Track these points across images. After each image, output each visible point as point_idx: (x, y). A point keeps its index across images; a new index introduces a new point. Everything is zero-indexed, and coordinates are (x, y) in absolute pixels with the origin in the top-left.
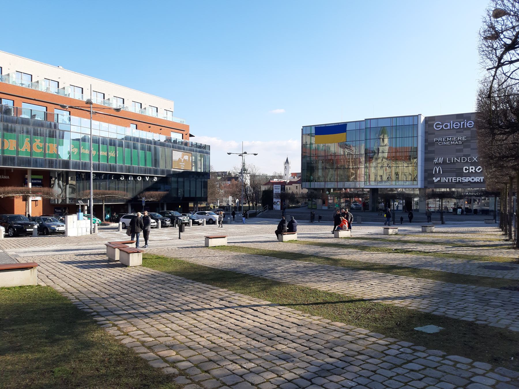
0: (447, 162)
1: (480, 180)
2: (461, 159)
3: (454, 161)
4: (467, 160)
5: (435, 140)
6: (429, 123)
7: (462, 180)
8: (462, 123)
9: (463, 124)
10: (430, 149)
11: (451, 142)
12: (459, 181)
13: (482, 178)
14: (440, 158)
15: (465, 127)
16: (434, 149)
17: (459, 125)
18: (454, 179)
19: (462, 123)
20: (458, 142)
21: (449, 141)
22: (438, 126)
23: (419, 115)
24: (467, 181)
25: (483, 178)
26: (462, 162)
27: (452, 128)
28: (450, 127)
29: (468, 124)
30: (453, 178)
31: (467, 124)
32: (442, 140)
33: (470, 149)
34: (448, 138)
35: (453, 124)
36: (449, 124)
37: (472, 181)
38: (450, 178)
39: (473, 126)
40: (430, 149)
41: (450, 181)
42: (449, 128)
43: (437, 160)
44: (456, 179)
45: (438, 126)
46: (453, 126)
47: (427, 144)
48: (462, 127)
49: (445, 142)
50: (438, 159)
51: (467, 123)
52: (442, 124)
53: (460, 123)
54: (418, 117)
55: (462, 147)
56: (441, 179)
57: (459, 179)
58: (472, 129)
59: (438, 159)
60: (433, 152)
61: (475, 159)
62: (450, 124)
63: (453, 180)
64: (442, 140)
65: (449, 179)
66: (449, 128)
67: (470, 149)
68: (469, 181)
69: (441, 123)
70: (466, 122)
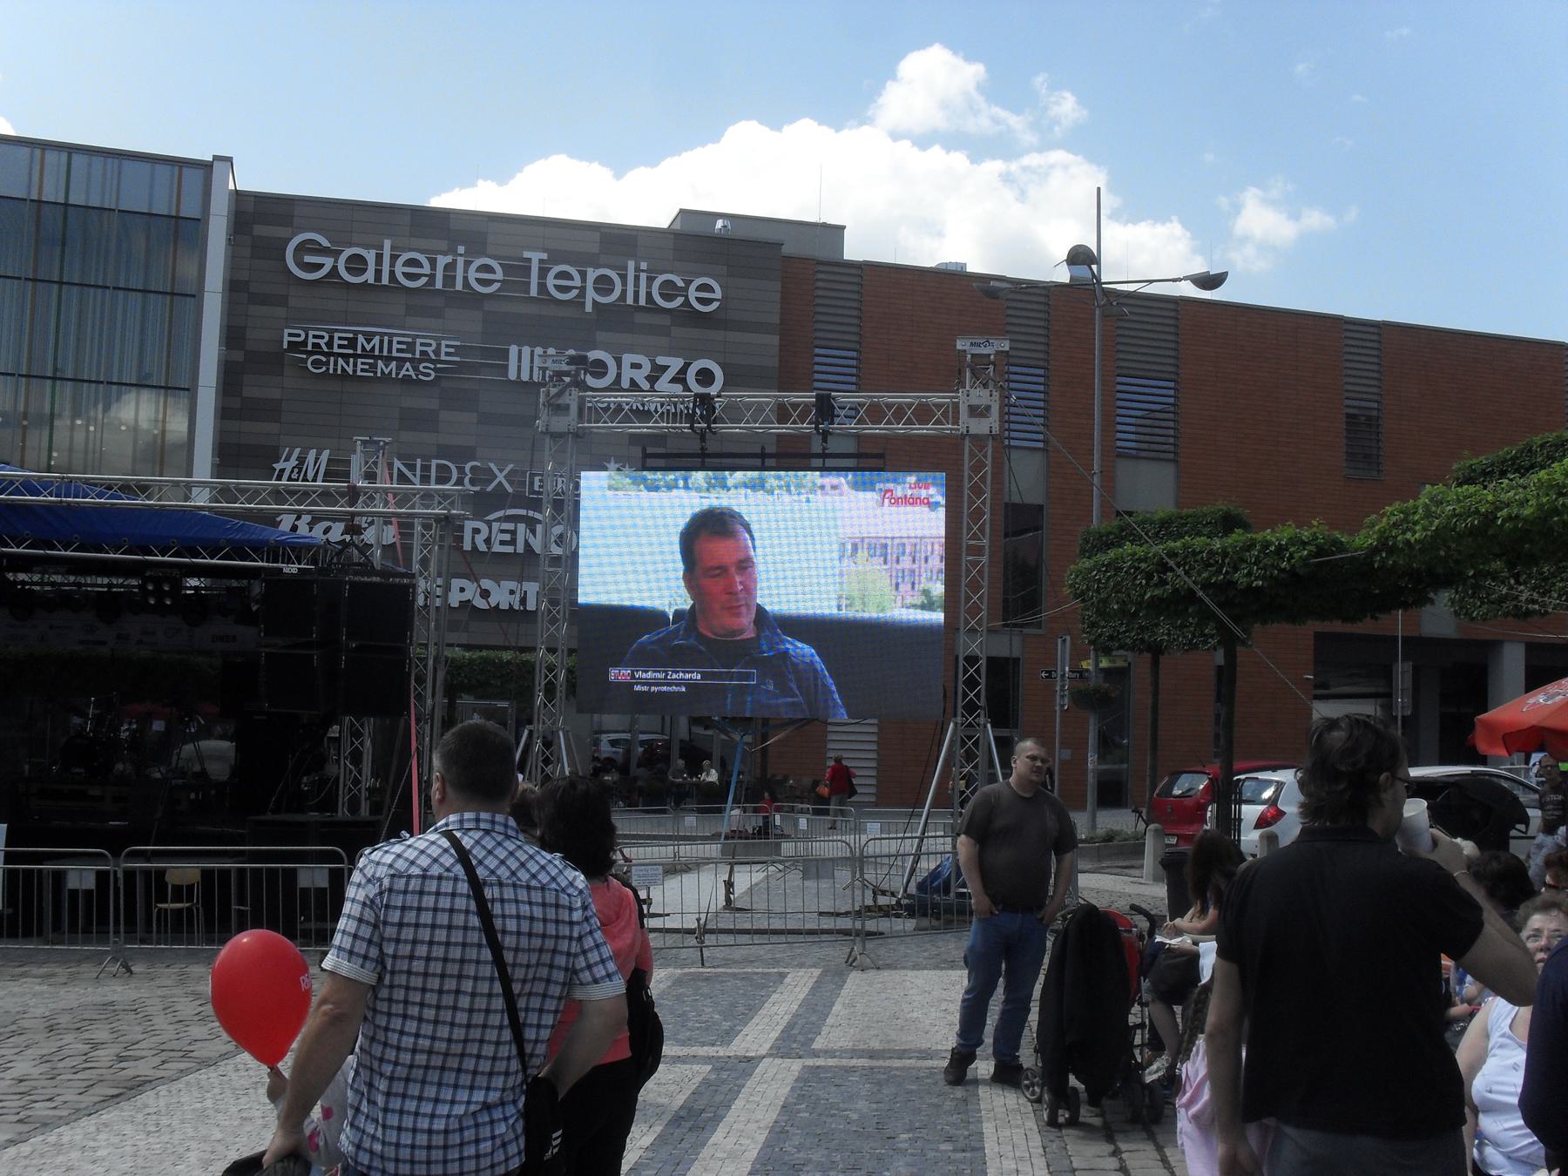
1: (523, 601)
2: (426, 468)
5: (286, 339)
6: (261, 230)
8: (442, 261)
9: (450, 267)
10: (256, 388)
11: (380, 363)
15: (459, 286)
16: (276, 394)
17: (427, 270)
19: (442, 261)
20: (416, 369)
21: (366, 354)
22: (308, 259)
23: (216, 157)
28: (378, 273)
31: (466, 271)
32: (330, 344)
34: (361, 339)
35: (394, 258)
36: (370, 256)
37: (480, 603)
39: (496, 286)
40: (256, 388)
42: (369, 276)
43: (293, 462)
45: (308, 259)
46: (392, 273)
47: (238, 356)
48: (439, 285)
49: (345, 357)
50: (301, 460)
51: (467, 264)
52: (338, 253)
53: (433, 263)
54: (206, 170)
55: (434, 404)
59: (301, 460)
60: (268, 410)
61: (501, 477)
62: (379, 257)
64: (330, 344)
66: (369, 276)
70: (461, 261)
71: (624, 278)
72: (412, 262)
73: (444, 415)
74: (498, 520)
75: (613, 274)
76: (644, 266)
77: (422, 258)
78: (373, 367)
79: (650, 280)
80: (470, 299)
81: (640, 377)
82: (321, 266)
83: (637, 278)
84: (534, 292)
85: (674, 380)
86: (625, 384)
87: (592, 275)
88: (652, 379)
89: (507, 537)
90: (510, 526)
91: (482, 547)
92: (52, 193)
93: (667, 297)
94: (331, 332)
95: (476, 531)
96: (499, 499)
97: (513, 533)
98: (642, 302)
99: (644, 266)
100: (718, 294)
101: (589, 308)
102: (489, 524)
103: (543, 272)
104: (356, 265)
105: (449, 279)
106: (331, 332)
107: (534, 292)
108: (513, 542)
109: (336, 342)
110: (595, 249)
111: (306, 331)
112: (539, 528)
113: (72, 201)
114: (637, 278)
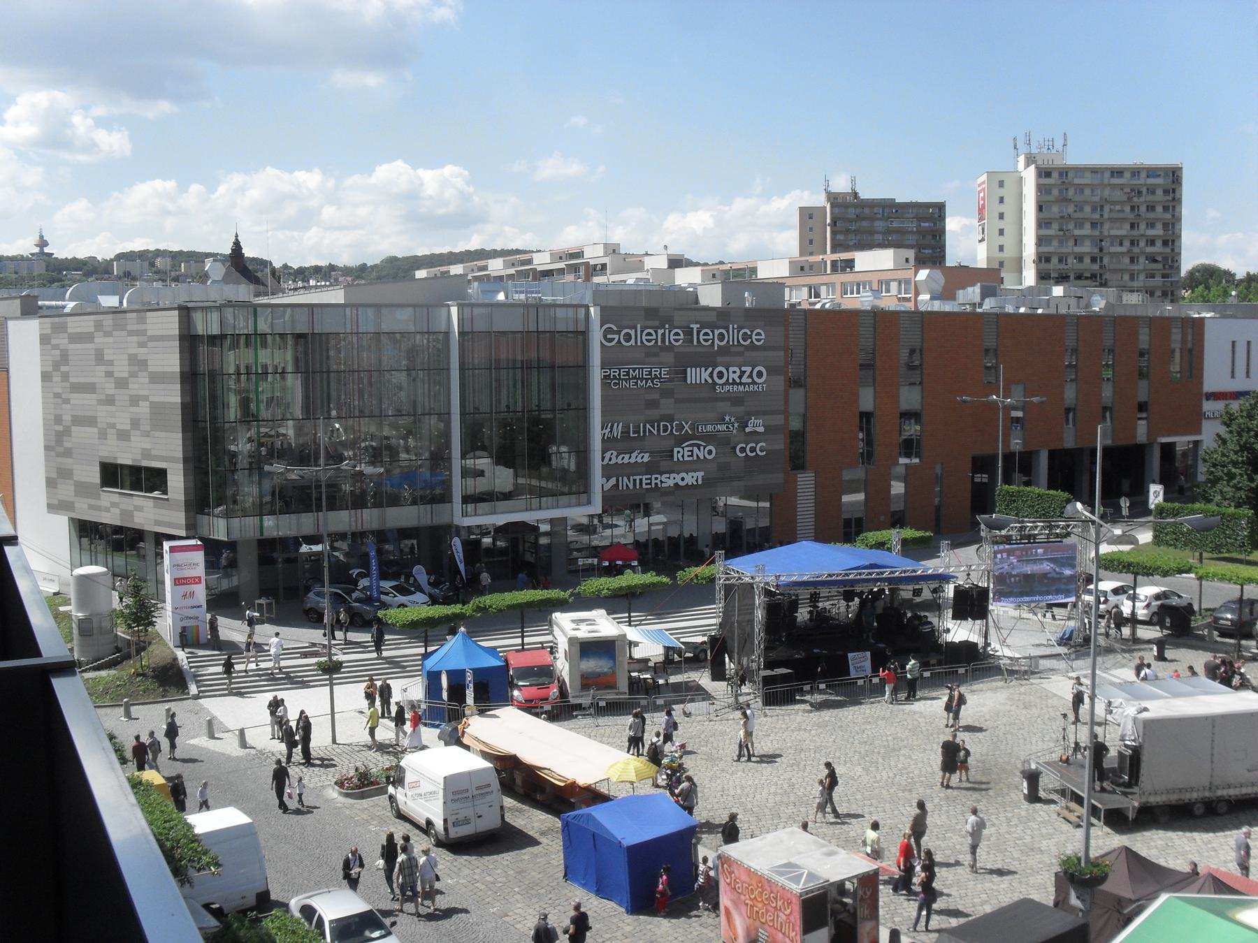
0: (632, 435)
1: (697, 481)
3: (644, 432)
4: (671, 431)
9: (663, 335)
12: (656, 484)
13: (700, 474)
14: (616, 424)
15: (667, 344)
18: (646, 479)
19: (660, 332)
20: (652, 382)
21: (635, 378)
24: (671, 483)
25: (702, 473)
26: (662, 434)
27: (639, 343)
28: (636, 343)
29: (672, 337)
30: (644, 477)
31: (669, 334)
32: (619, 375)
33: (672, 401)
35: (642, 332)
36: (632, 332)
37: (682, 484)
38: (638, 478)
41: (638, 487)
42: (633, 342)
43: (609, 430)
44: (650, 479)
45: (609, 336)
48: (659, 344)
49: (626, 380)
51: (670, 332)
52: (619, 332)
56: (618, 480)
57: (656, 479)
58: (676, 350)
61: (686, 427)
62: (636, 331)
63: (644, 481)
64: (619, 375)
65: (635, 480)
66: (633, 342)
67: (673, 400)
69: (615, 329)
70: (667, 331)
71: (728, 332)
73: (662, 401)
75: (724, 331)
76: (735, 326)
78: (637, 383)
79: (738, 332)
80: (671, 347)
81: (736, 376)
83: (733, 331)
84: (695, 343)
85: (748, 377)
86: (731, 381)
87: (717, 332)
88: (740, 377)
89: (690, 453)
90: (691, 449)
91: (681, 459)
94: (620, 370)
95: (678, 452)
96: (687, 437)
97: (692, 451)
98: (736, 343)
99: (735, 326)
100: (763, 337)
101: (716, 348)
102: (683, 448)
103: (698, 333)
104: (628, 337)
105: (663, 340)
106: (620, 370)
107: (695, 343)
108: (692, 455)
109: (622, 374)
110: (714, 319)
111: (610, 369)
112: (702, 448)
114: (733, 331)
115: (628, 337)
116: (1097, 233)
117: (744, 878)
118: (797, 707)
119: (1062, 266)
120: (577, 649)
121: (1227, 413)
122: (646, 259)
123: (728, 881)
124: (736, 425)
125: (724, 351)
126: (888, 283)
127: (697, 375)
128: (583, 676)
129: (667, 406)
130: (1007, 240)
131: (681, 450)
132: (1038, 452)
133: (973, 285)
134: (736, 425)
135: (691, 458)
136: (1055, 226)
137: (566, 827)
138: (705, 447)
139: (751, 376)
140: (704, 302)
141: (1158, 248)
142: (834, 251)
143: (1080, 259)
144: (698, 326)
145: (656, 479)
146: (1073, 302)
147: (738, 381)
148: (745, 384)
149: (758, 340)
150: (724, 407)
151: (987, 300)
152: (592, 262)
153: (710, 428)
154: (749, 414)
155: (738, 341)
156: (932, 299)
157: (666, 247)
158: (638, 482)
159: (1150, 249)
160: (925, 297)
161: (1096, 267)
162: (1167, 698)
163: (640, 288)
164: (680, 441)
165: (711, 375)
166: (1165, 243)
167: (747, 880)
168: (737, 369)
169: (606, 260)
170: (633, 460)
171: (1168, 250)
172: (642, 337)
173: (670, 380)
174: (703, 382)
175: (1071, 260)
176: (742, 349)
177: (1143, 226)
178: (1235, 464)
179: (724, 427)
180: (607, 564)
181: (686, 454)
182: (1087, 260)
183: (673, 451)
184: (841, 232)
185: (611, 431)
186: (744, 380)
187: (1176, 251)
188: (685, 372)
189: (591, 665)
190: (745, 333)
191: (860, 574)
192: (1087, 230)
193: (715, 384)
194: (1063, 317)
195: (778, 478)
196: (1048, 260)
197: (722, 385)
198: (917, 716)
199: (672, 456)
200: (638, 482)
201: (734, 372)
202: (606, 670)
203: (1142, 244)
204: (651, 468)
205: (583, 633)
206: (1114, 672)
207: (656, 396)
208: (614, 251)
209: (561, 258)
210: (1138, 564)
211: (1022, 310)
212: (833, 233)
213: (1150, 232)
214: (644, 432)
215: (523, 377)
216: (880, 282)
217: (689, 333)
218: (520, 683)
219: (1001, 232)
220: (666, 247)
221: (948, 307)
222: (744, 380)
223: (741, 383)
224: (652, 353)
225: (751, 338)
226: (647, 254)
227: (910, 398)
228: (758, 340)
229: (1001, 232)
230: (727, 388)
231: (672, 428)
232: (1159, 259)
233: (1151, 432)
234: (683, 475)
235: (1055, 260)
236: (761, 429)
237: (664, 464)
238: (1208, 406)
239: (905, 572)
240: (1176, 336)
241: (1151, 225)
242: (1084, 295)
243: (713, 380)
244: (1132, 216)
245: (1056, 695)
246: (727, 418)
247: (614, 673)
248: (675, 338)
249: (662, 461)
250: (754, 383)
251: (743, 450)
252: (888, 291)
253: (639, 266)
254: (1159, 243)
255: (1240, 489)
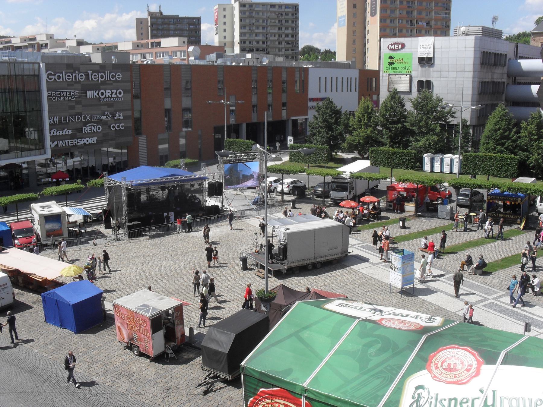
1: (94, 141)
2: (75, 118)
3: (69, 120)
7: (78, 142)
8: (74, 75)
9: (75, 76)
12: (75, 143)
13: (95, 138)
15: (77, 80)
17: (71, 77)
19: (74, 75)
21: (63, 96)
24: (82, 143)
25: (96, 138)
27: (64, 80)
29: (79, 77)
30: (70, 141)
32: (56, 95)
33: (80, 106)
35: (65, 75)
36: (61, 75)
37: (87, 143)
38: (67, 141)
41: (67, 145)
42: (61, 79)
43: (52, 120)
44: (73, 141)
45: (50, 77)
48: (74, 80)
50: (53, 119)
51: (78, 75)
52: (54, 75)
56: (58, 143)
57: (75, 141)
59: (53, 119)
61: (88, 118)
63: (70, 143)
64: (56, 95)
66: (61, 79)
68: (85, 143)
70: (77, 74)
71: (105, 74)
72: (69, 76)
73: (76, 106)
74: (89, 126)
75: (103, 74)
77: (70, 74)
78: (64, 98)
79: (110, 74)
80: (79, 81)
82: (52, 78)
84: (90, 80)
86: (107, 96)
87: (100, 75)
88: (111, 95)
90: (90, 127)
91: (86, 132)
92: (13, 73)
93: (113, 78)
94: (56, 92)
95: (85, 129)
96: (88, 122)
97: (91, 128)
100: (121, 76)
103: (92, 75)
106: (56, 92)
107: (90, 80)
108: (91, 130)
112: (95, 127)
113: (16, 74)
115: (59, 77)
116: (265, 31)
117: (125, 313)
118: (143, 238)
119: (251, 45)
120: (43, 219)
121: (318, 106)
122: (12, 39)
123: (118, 315)
124: (110, 116)
125: (104, 83)
126: (176, 52)
127: (92, 94)
128: (47, 231)
129: (79, 109)
130: (227, 34)
131: (86, 128)
132: (241, 124)
133: (213, 53)
134: (110, 116)
135: (91, 132)
136: (247, 28)
137: (44, 299)
138: (97, 126)
139: (116, 94)
140: (93, 61)
141: (290, 38)
142: (152, 37)
143: (258, 43)
144: (91, 72)
145: (75, 141)
146: (255, 60)
147: (110, 96)
148: (113, 98)
149: (119, 78)
150: (105, 108)
151: (219, 60)
152: (41, 43)
153: (98, 118)
154: (116, 111)
155: (110, 79)
156: (195, 59)
157: (75, 36)
158: (67, 143)
159: (286, 39)
160: (192, 58)
161: (265, 46)
162: (296, 223)
163: (64, 55)
164: (85, 124)
165: (98, 94)
166: (293, 36)
167: (127, 314)
168: (110, 91)
169: (47, 42)
170: (64, 133)
171: (294, 39)
172: (65, 77)
173: (79, 97)
174: (95, 97)
175: (254, 43)
176: (112, 82)
177: (283, 29)
178: (321, 127)
179: (105, 117)
180: (55, 180)
181: (88, 129)
182: (261, 43)
183: (82, 129)
184: (155, 30)
185: (53, 121)
186: (113, 96)
187: (297, 39)
188: (86, 93)
189: (50, 226)
190: (113, 75)
191: (167, 179)
192: (261, 30)
193: (100, 98)
194: (251, 67)
195: (130, 139)
196: (244, 43)
197: (103, 98)
198: (195, 238)
199: (82, 131)
200: (67, 143)
201: (109, 92)
202: (57, 228)
203: (283, 36)
204: (73, 137)
205: (46, 212)
206: (275, 214)
207: (74, 104)
208: (51, 37)
209: (25, 40)
210: (284, 170)
211: (234, 64)
212: (152, 30)
213: (286, 32)
214: (69, 120)
215: (9, 96)
216: (173, 52)
217: (87, 75)
218: (18, 237)
219: (225, 30)
220: (75, 36)
221: (202, 63)
222: (113, 96)
223: (112, 97)
224: (70, 85)
225: (115, 76)
226: (67, 39)
227: (186, 102)
228: (119, 78)
229: (225, 30)
230: (105, 99)
231: (81, 118)
232: (290, 43)
233: (288, 115)
234: (87, 139)
235: (247, 43)
236: (122, 118)
237: (79, 134)
238: (311, 104)
239: (186, 177)
240: (297, 75)
241: (287, 28)
242: (260, 57)
243: (99, 96)
244: (279, 25)
245: (252, 226)
246: (106, 113)
247: (61, 228)
248: (81, 77)
249: (78, 133)
250: (118, 97)
251: (114, 127)
252: (176, 56)
253: (63, 45)
254: (290, 36)
255: (323, 137)
